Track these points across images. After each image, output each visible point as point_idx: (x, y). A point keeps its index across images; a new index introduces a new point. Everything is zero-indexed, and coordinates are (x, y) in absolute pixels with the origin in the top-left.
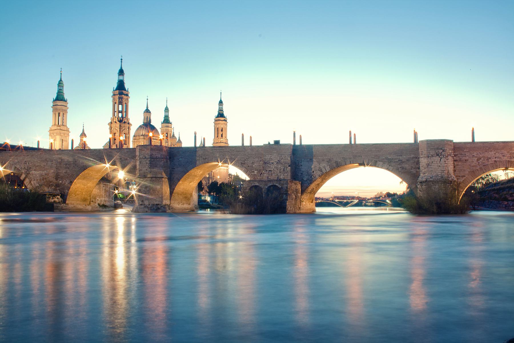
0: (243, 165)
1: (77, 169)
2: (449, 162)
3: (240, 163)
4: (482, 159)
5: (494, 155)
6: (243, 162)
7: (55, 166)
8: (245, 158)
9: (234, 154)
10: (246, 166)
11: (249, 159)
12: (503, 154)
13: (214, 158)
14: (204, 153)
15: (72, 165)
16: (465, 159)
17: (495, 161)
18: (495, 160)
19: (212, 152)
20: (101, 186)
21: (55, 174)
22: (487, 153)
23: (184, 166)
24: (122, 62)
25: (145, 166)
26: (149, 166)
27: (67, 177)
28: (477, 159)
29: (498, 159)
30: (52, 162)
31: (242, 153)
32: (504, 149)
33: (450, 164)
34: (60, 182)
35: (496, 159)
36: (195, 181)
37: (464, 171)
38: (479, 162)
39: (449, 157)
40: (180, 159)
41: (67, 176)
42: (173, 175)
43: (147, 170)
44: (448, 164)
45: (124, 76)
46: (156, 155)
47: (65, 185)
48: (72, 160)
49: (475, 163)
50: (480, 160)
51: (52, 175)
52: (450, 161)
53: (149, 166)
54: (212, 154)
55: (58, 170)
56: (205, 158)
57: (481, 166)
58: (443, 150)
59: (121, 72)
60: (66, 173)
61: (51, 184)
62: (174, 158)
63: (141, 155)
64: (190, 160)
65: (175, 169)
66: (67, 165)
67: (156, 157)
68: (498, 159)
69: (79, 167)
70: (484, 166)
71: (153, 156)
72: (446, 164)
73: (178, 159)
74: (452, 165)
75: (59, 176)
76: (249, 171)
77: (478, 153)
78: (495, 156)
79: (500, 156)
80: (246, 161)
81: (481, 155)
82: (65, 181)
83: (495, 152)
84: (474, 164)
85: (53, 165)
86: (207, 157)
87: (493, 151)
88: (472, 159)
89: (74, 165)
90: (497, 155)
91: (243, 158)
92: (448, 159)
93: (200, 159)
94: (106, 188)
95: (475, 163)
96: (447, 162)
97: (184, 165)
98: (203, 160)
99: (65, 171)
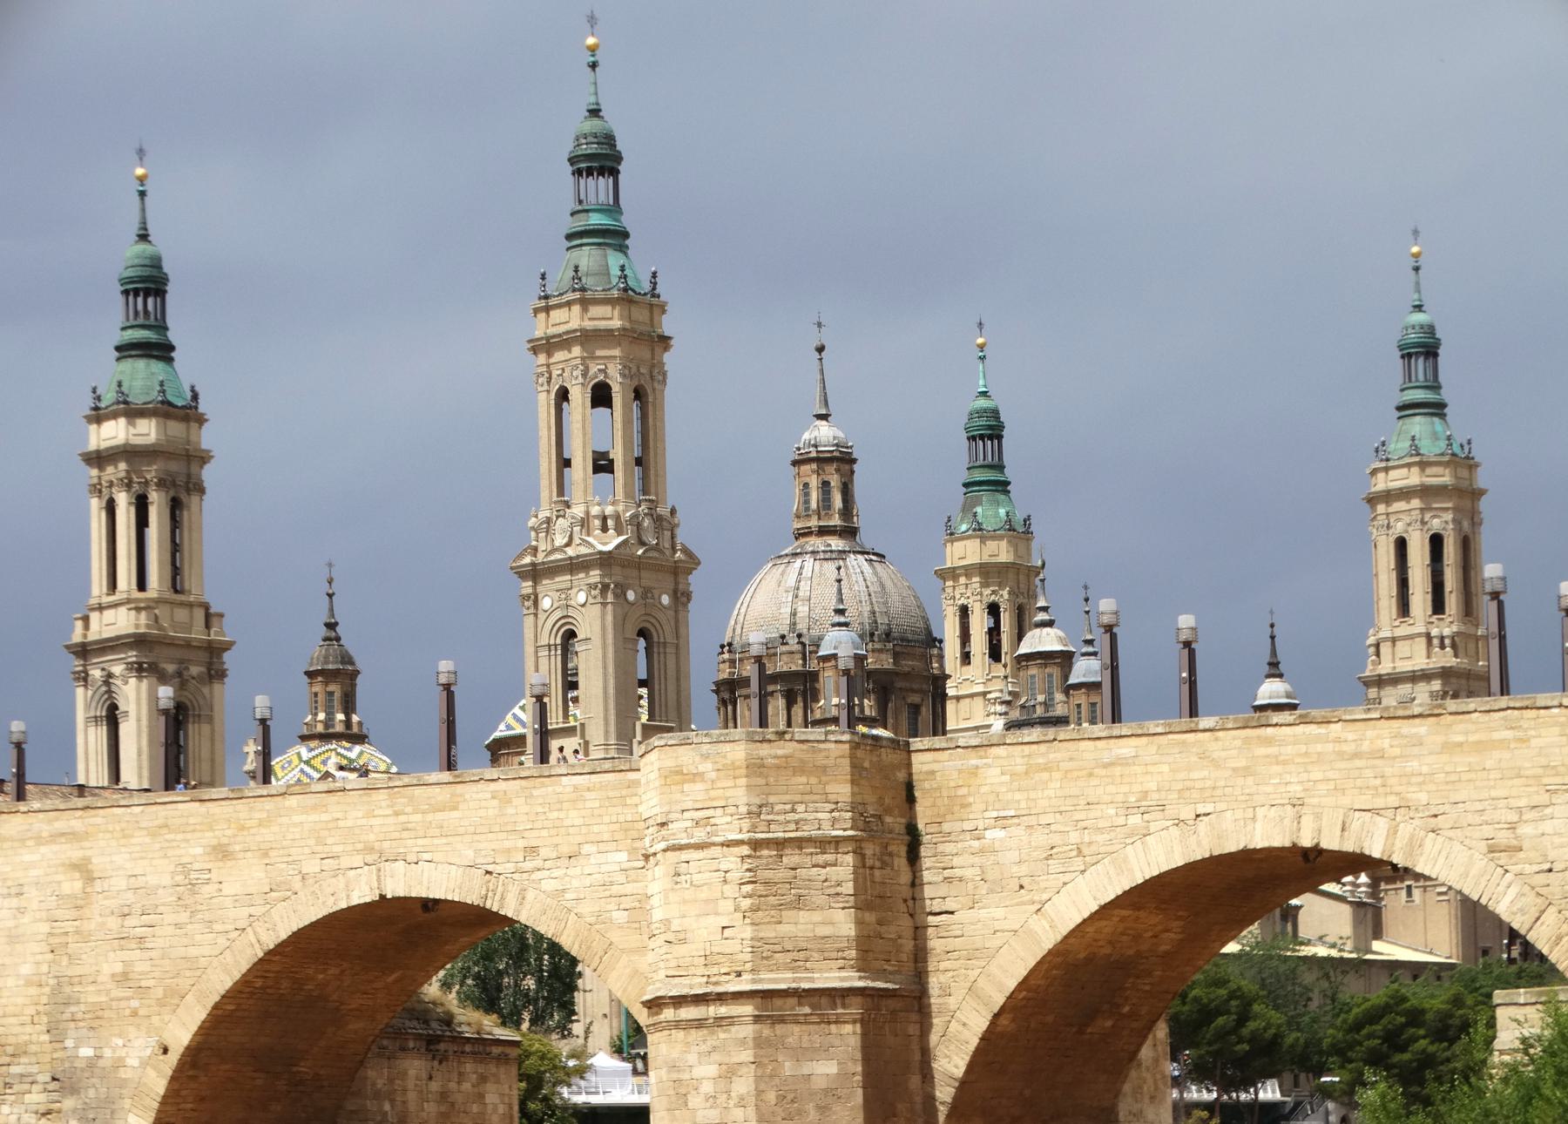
0: (1503, 858)
1: (206, 951)
3: (1483, 846)
6: (1503, 837)
7: (44, 928)
8: (1522, 803)
9: (1425, 769)
10: (1528, 869)
11: (1548, 811)
13: (1260, 812)
14: (1182, 775)
15: (170, 918)
19: (1242, 763)
20: (412, 1072)
21: (47, 990)
23: (1022, 887)
25: (707, 901)
26: (746, 903)
27: (135, 1014)
30: (14, 902)
31: (1489, 764)
34: (86, 1052)
36: (1126, 1009)
40: (988, 834)
41: (135, 1003)
42: (942, 966)
43: (727, 932)
46: (793, 811)
47: (123, 1074)
48: (167, 880)
51: (20, 1000)
53: (746, 903)
54: (1250, 780)
55: (65, 961)
56: (1187, 813)
60: (123, 978)
61: (14, 1070)
62: (946, 827)
63: (672, 816)
64: (1074, 837)
65: (952, 913)
66: (130, 922)
67: (797, 823)
69: (218, 927)
71: (769, 822)
73: (977, 834)
75: (73, 1009)
76: (1552, 910)
80: (1525, 830)
82: (120, 1042)
85: (26, 920)
86: (1209, 808)
89: (183, 917)
91: (1502, 803)
93: (1153, 827)
94: (453, 1085)
97: (1025, 882)
98: (1175, 831)
99: (119, 968)
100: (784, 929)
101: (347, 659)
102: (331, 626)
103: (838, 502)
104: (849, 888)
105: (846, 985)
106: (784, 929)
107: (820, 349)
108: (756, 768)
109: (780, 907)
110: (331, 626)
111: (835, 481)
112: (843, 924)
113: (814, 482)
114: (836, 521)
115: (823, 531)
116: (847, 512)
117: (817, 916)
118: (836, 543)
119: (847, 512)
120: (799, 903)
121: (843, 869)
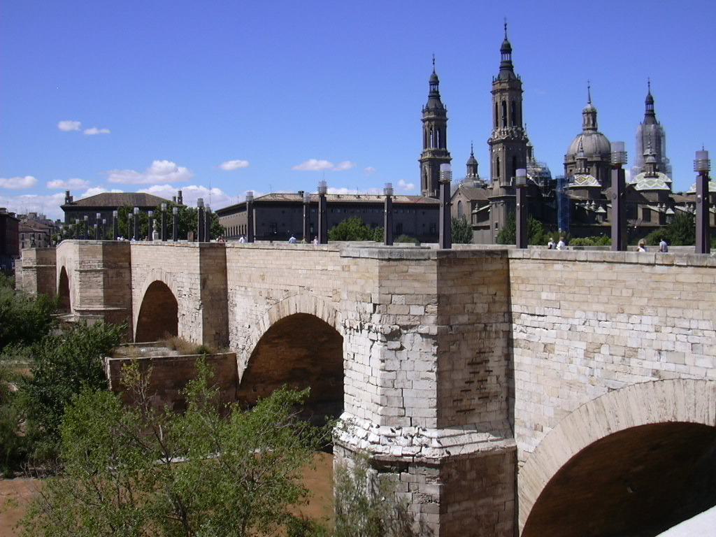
2: (406, 366)
4: (605, 350)
5: (654, 336)
12: (696, 340)
16: (545, 342)
17: (656, 373)
18: (657, 366)
22: (622, 317)
24: (506, 29)
28: (583, 345)
29: (672, 367)
32: (701, 305)
33: (410, 375)
35: (664, 365)
37: (540, 402)
38: (592, 364)
39: (407, 338)
44: (400, 378)
45: (510, 53)
49: (579, 372)
50: (598, 358)
52: (415, 356)
57: (601, 390)
58: (375, 305)
59: (507, 49)
68: (672, 367)
70: (610, 390)
72: (392, 375)
74: (428, 379)
77: (590, 315)
78: (657, 345)
79: (679, 348)
81: (599, 331)
83: (656, 320)
84: (575, 376)
87: (650, 311)
88: (567, 342)
90: (668, 338)
92: (402, 348)
95: (579, 372)
96: (397, 363)
100: (87, 294)
101: (475, 161)
102: (472, 155)
103: (591, 122)
104: (102, 283)
105: (99, 309)
106: (87, 294)
107: (589, 87)
108: (81, 250)
109: (86, 288)
110: (472, 155)
111: (591, 118)
112: (100, 293)
113: (586, 118)
114: (591, 127)
115: (588, 129)
116: (594, 124)
117: (94, 291)
118: (590, 132)
119: (594, 124)
120: (90, 287)
121: (100, 279)
